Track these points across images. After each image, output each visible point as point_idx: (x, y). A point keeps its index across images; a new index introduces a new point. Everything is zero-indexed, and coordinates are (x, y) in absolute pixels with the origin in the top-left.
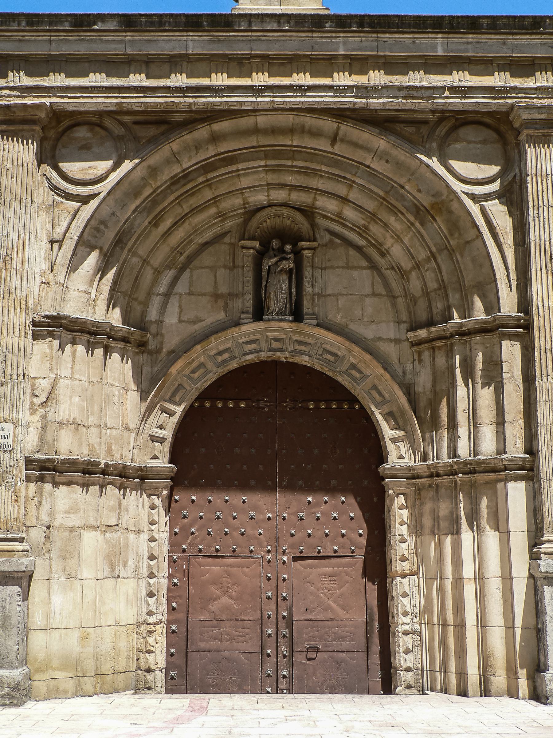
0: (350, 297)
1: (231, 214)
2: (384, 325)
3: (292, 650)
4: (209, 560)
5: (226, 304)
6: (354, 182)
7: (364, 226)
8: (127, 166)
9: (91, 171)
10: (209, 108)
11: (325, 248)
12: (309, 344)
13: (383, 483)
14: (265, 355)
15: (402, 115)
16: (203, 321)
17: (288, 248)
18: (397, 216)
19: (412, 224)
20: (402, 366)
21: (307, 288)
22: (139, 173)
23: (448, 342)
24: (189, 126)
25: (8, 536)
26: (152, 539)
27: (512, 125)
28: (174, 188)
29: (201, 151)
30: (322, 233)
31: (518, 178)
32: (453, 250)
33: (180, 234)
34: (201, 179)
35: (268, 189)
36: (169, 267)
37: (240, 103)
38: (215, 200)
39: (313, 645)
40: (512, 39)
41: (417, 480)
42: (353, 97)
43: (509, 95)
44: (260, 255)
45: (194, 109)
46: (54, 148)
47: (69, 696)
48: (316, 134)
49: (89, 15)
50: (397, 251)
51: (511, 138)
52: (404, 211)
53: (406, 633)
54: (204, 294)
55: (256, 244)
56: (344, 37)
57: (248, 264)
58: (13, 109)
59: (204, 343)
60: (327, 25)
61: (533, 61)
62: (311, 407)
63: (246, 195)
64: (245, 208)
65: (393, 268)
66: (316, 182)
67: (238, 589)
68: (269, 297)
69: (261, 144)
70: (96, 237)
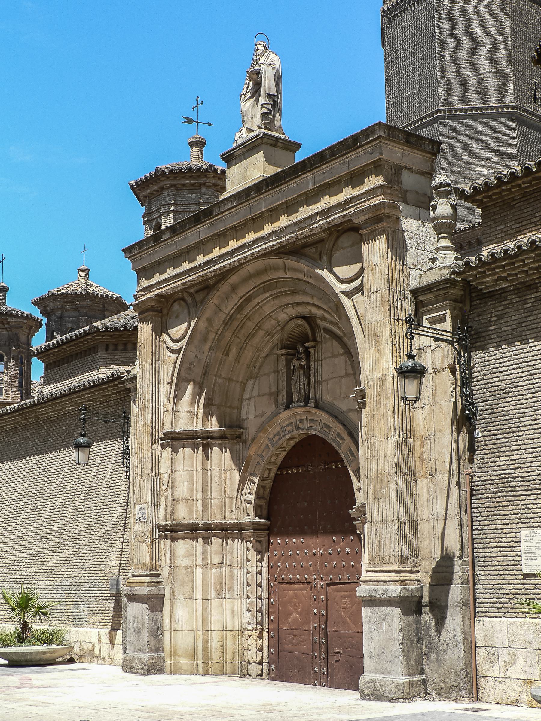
1: (274, 331)
4: (288, 585)
5: (275, 399)
15: (309, 240)
21: (312, 379)
22: (203, 325)
26: (249, 572)
36: (250, 378)
38: (258, 326)
43: (351, 205)
47: (188, 673)
48: (276, 269)
54: (264, 395)
60: (252, 194)
64: (279, 325)
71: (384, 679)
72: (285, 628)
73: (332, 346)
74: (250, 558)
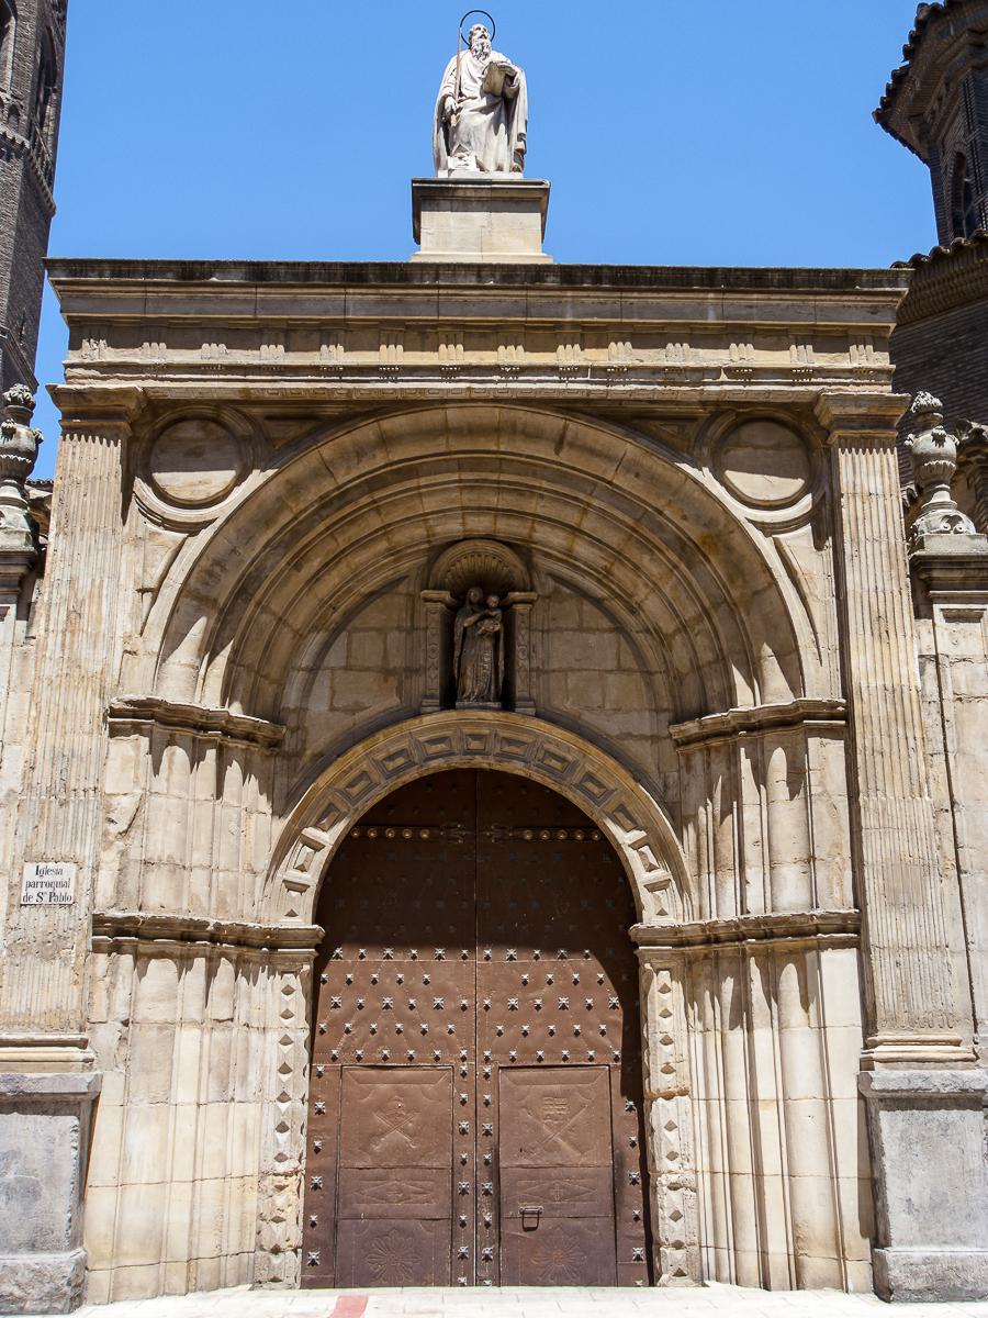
0: (585, 673)
1: (409, 551)
2: (636, 714)
3: (498, 1217)
5: (400, 683)
6: (589, 505)
7: (605, 568)
8: (256, 478)
9: (202, 488)
10: (375, 396)
11: (547, 601)
12: (524, 743)
13: (635, 952)
14: (457, 761)
15: (660, 408)
16: (366, 708)
17: (493, 600)
18: (653, 554)
19: (675, 567)
20: (662, 776)
21: (521, 660)
22: (273, 490)
23: (730, 740)
24: (347, 424)
25: (62, 1037)
26: (286, 1041)
27: (818, 423)
28: (324, 513)
29: (364, 459)
30: (543, 580)
31: (828, 494)
32: (735, 604)
33: (332, 580)
34: (364, 500)
35: (463, 514)
36: (315, 628)
37: (422, 391)
38: (386, 530)
39: (531, 1208)
40: (815, 301)
41: (687, 948)
42: (587, 382)
43: (813, 380)
44: (452, 612)
45: (354, 398)
46: (148, 452)
47: (149, 1293)
49: (202, 263)
50: (653, 605)
51: (817, 442)
52: (663, 547)
53: (674, 1187)
54: (367, 669)
55: (446, 595)
56: (573, 297)
57: (433, 625)
58: (90, 397)
59: (368, 742)
60: (548, 280)
61: (846, 331)
62: (528, 837)
63: (431, 523)
64: (429, 542)
65: (647, 631)
66: (533, 505)
67: (416, 1117)
68: (465, 673)
69: (453, 449)
70: (207, 584)
71: (961, 1255)
72: (361, 1165)
73: (580, 612)
74: (292, 1009)
